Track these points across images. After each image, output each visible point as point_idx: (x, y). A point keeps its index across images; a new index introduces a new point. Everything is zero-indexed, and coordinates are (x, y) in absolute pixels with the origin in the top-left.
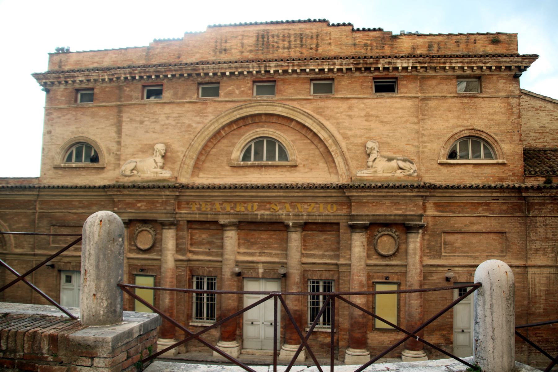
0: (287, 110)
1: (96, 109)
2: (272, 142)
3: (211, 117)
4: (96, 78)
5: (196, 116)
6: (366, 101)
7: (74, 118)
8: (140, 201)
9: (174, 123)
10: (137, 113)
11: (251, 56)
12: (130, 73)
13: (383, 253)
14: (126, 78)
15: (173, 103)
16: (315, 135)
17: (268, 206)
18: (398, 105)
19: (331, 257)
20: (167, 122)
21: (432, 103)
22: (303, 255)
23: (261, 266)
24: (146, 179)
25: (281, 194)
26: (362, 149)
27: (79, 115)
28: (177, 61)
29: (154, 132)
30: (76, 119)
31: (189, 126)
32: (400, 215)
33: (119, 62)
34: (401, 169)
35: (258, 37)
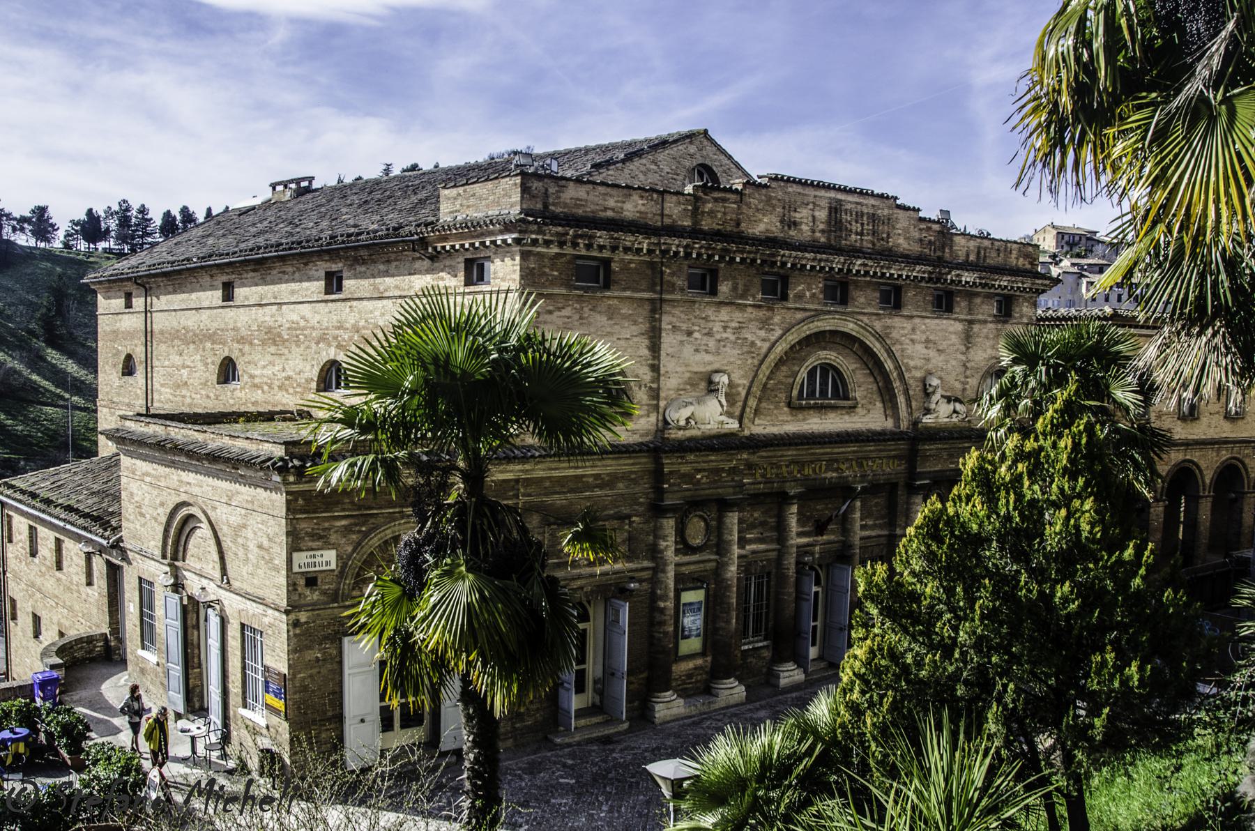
0: (857, 328)
1: (616, 302)
2: (826, 368)
3: (778, 332)
6: (927, 321)
7: (577, 317)
8: (699, 471)
9: (732, 338)
10: (683, 316)
14: (677, 253)
16: (879, 364)
17: (835, 465)
18: (951, 329)
19: (881, 527)
20: (725, 335)
21: (976, 328)
22: (863, 527)
24: (708, 433)
26: (920, 384)
27: (586, 309)
29: (707, 352)
30: (581, 318)
31: (753, 344)
33: (650, 216)
34: (955, 411)
35: (830, 208)
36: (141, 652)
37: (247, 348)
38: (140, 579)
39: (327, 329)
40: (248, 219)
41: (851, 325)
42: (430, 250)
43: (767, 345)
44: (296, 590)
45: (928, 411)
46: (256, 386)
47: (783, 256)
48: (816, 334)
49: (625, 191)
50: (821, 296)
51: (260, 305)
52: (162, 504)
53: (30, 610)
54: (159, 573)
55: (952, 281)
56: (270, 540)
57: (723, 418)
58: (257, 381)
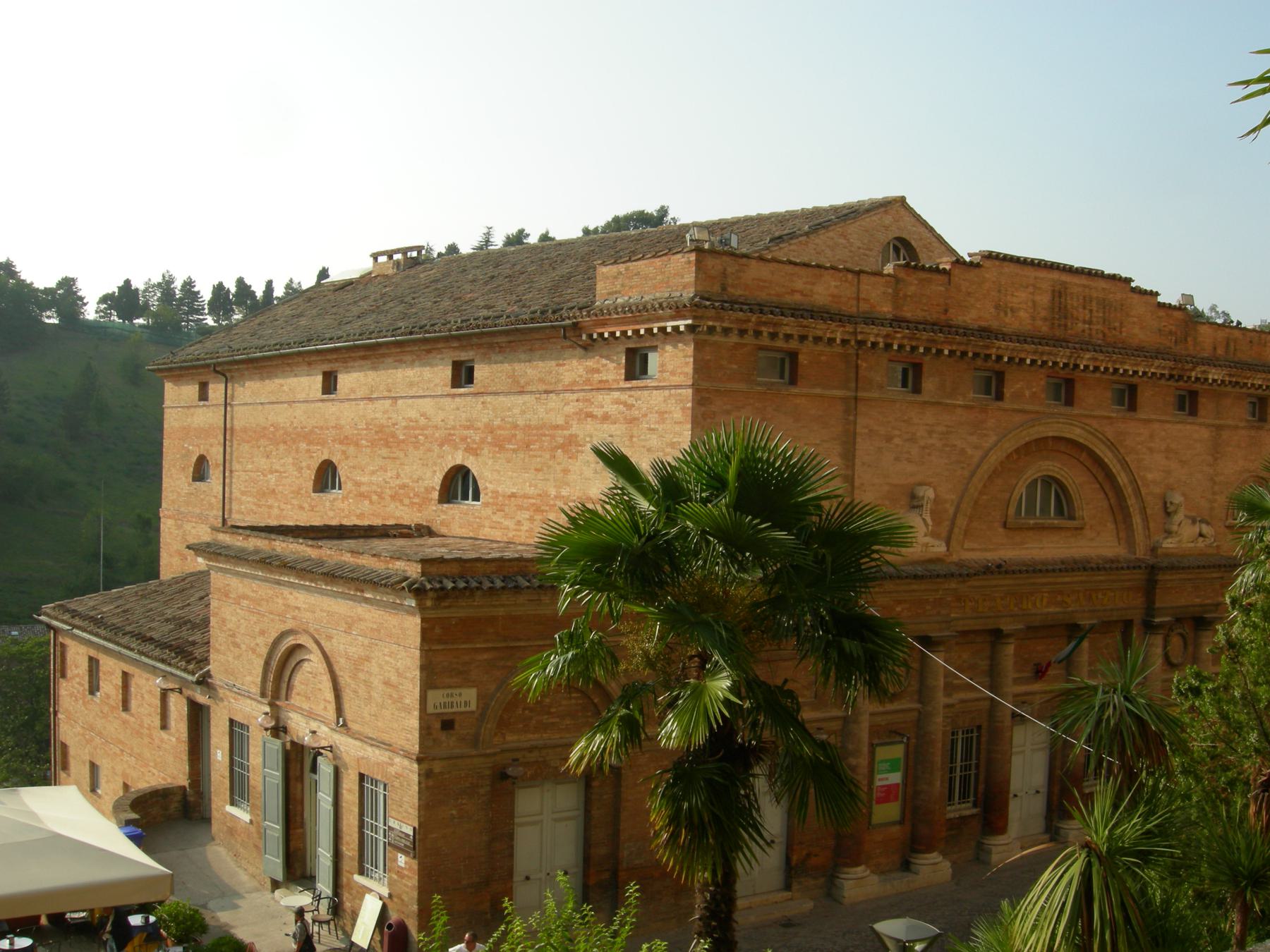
2: (1049, 481)
3: (993, 439)
4: (819, 333)
5: (972, 434)
6: (1168, 426)
8: (899, 602)
11: (1045, 329)
12: (887, 336)
13: (1175, 661)
14: (874, 344)
15: (939, 403)
16: (1110, 477)
17: (1059, 598)
20: (930, 441)
21: (1225, 434)
23: (1038, 697)
25: (1083, 578)
28: (943, 317)
29: (909, 460)
31: (963, 451)
32: (1201, 606)
34: (1201, 535)
36: (229, 809)
37: (351, 450)
38: (232, 721)
39: (454, 428)
40: (347, 296)
41: (1078, 431)
42: (584, 337)
43: (978, 454)
44: (430, 734)
45: (1169, 533)
46: (362, 496)
47: (999, 348)
48: (1036, 440)
49: (817, 271)
50: (1043, 396)
51: (370, 399)
52: (262, 633)
53: (87, 758)
54: (255, 713)
55: (1197, 379)
56: (400, 675)
57: (928, 539)
58: (363, 489)
